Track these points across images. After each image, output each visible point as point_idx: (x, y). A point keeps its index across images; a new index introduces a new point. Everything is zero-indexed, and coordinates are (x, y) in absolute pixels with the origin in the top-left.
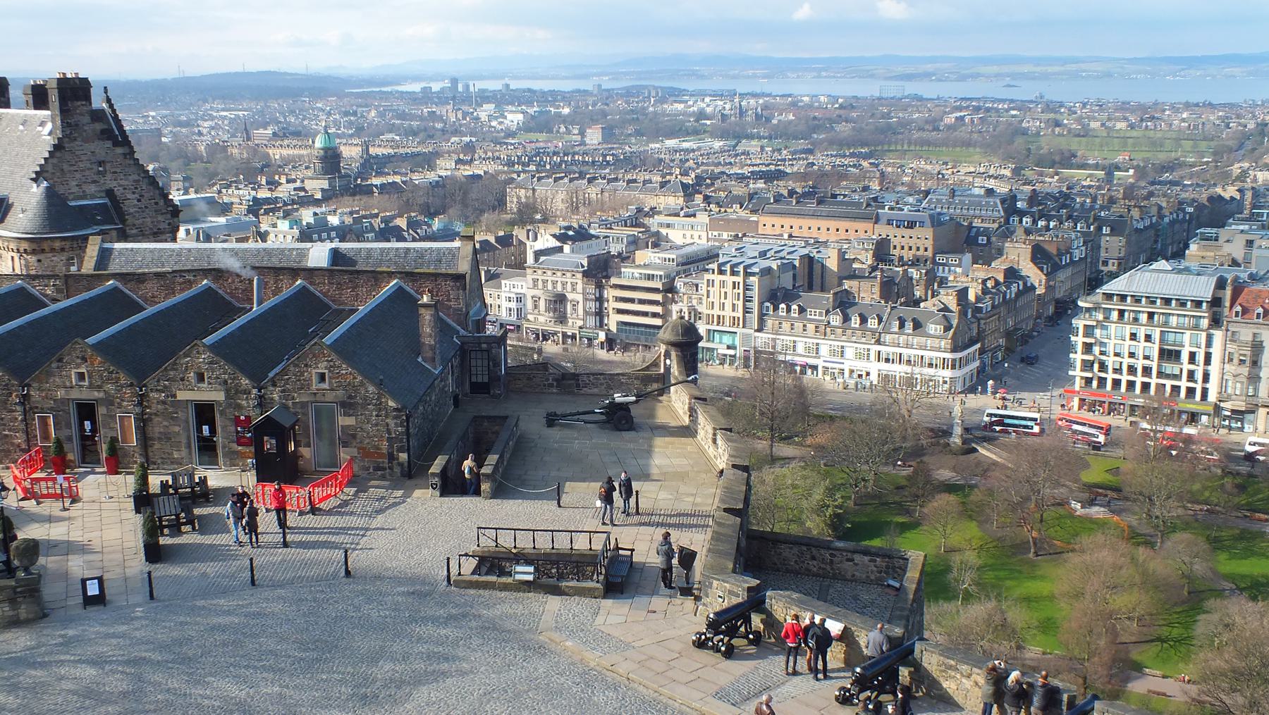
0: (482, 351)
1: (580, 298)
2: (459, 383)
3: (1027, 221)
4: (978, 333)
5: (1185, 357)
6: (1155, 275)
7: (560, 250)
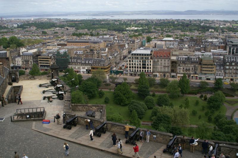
0: (13, 73)
1: (32, 61)
2: (9, 80)
3: (117, 41)
4: (110, 63)
5: (147, 65)
6: (140, 50)
7: (27, 51)
